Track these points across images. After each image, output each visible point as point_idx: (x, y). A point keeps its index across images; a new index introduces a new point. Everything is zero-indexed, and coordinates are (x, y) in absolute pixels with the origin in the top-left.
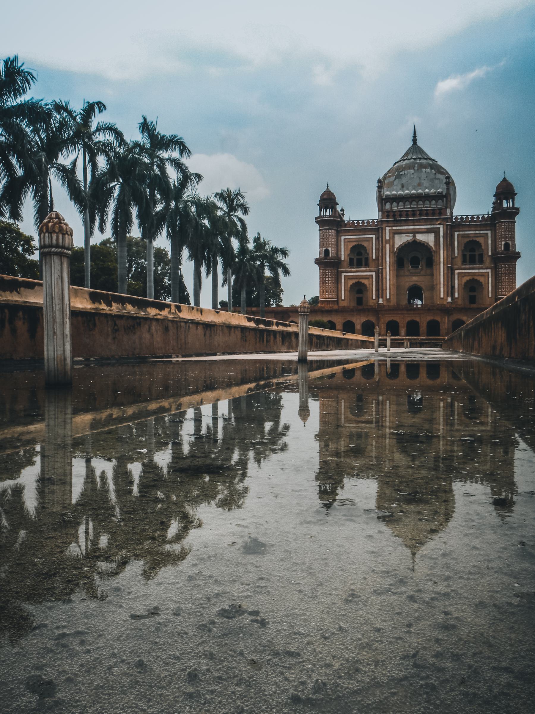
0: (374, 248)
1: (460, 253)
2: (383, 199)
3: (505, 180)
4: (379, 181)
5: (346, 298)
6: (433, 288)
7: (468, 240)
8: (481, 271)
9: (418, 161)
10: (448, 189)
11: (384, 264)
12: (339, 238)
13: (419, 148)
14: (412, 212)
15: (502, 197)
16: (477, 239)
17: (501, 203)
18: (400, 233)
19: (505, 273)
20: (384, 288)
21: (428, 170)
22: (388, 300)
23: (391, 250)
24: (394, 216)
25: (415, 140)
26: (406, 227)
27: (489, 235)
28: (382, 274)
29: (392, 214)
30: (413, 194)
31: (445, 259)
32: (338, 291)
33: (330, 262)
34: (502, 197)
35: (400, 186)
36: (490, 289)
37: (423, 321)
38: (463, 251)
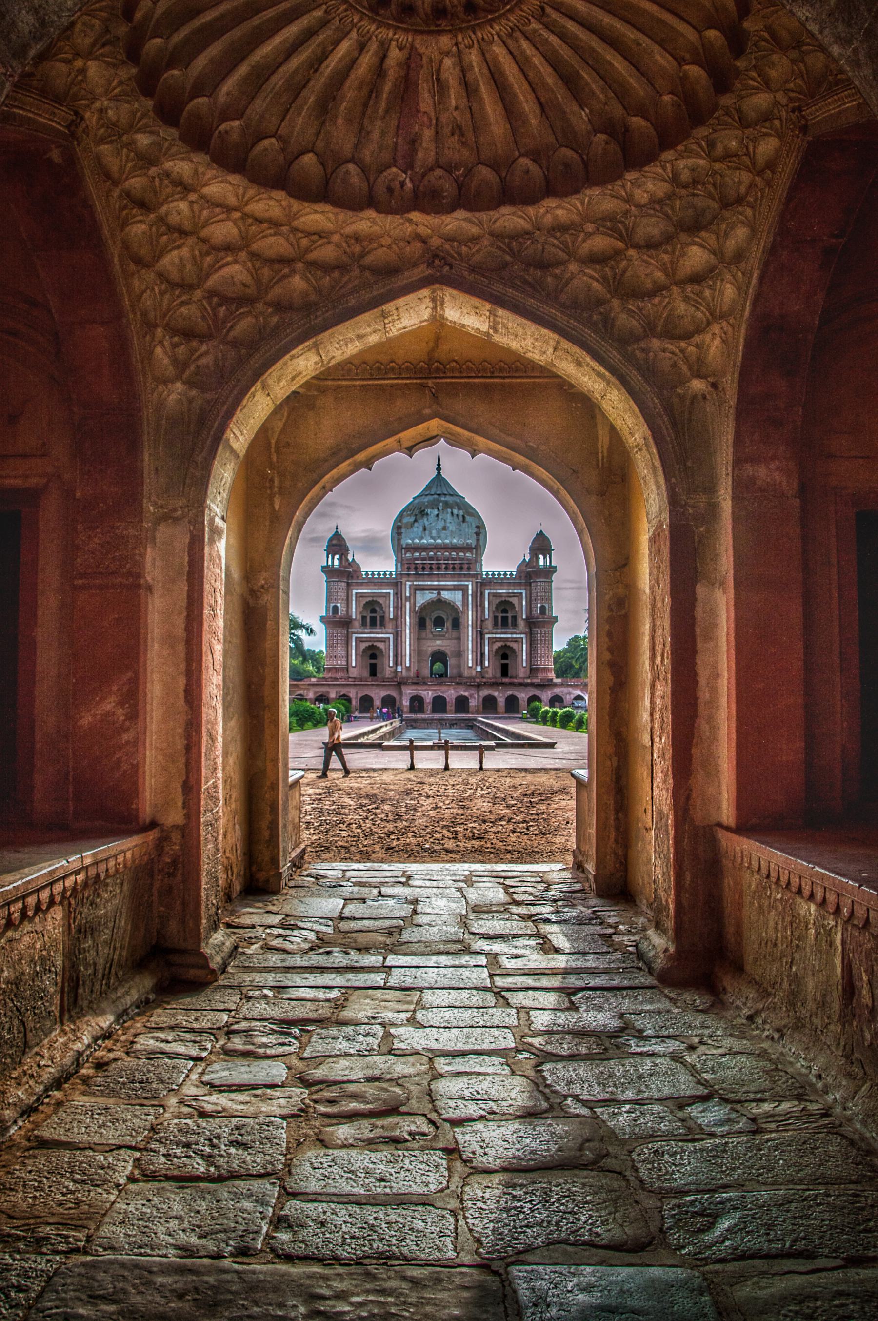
4: (399, 528)
6: (459, 654)
7: (499, 600)
10: (478, 540)
16: (511, 600)
17: (538, 559)
18: (422, 589)
22: (408, 669)
24: (416, 569)
25: (439, 469)
30: (438, 544)
32: (348, 656)
35: (421, 529)
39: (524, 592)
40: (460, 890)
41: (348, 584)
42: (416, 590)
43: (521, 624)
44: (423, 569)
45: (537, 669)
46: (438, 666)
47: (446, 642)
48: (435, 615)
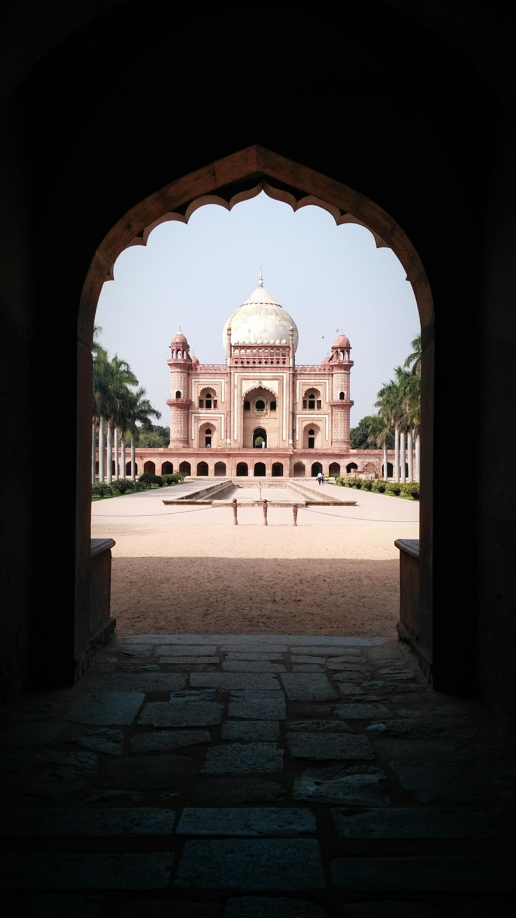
14: (259, 360)
16: (316, 388)
21: (273, 317)
22: (236, 441)
24: (242, 362)
28: (230, 416)
29: (241, 360)
33: (182, 404)
34: (339, 350)
37: (269, 463)
38: (303, 398)
39: (327, 381)
40: (278, 676)
41: (189, 374)
44: (248, 363)
46: (259, 438)
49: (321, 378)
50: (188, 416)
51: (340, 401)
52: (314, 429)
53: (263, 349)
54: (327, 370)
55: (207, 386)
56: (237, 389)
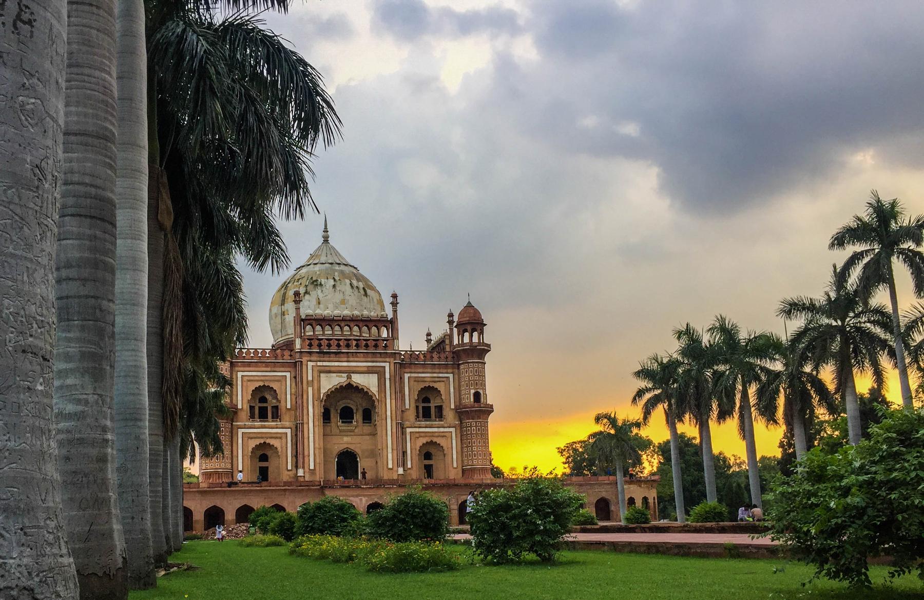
0: (289, 393)
1: (413, 405)
2: (302, 320)
3: (469, 306)
5: (246, 469)
6: (375, 454)
7: (422, 385)
8: (442, 430)
9: (337, 267)
11: (305, 417)
12: (234, 374)
13: (332, 247)
15: (469, 328)
16: (436, 385)
19: (477, 434)
20: (306, 453)
21: (355, 282)
22: (313, 472)
23: (316, 396)
24: (320, 345)
26: (336, 364)
27: (451, 380)
28: (303, 431)
29: (317, 342)
31: (394, 412)
35: (314, 302)
36: (455, 457)
39: (451, 376)
41: (232, 363)
42: (320, 372)
43: (450, 416)
44: (329, 346)
45: (473, 470)
47: (357, 439)
48: (342, 404)
49: (441, 371)
50: (232, 433)
51: (476, 405)
52: (432, 450)
53: (352, 325)
54: (450, 358)
55: (261, 384)
56: (313, 386)
